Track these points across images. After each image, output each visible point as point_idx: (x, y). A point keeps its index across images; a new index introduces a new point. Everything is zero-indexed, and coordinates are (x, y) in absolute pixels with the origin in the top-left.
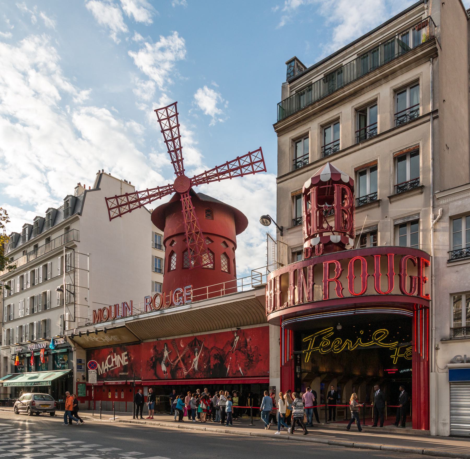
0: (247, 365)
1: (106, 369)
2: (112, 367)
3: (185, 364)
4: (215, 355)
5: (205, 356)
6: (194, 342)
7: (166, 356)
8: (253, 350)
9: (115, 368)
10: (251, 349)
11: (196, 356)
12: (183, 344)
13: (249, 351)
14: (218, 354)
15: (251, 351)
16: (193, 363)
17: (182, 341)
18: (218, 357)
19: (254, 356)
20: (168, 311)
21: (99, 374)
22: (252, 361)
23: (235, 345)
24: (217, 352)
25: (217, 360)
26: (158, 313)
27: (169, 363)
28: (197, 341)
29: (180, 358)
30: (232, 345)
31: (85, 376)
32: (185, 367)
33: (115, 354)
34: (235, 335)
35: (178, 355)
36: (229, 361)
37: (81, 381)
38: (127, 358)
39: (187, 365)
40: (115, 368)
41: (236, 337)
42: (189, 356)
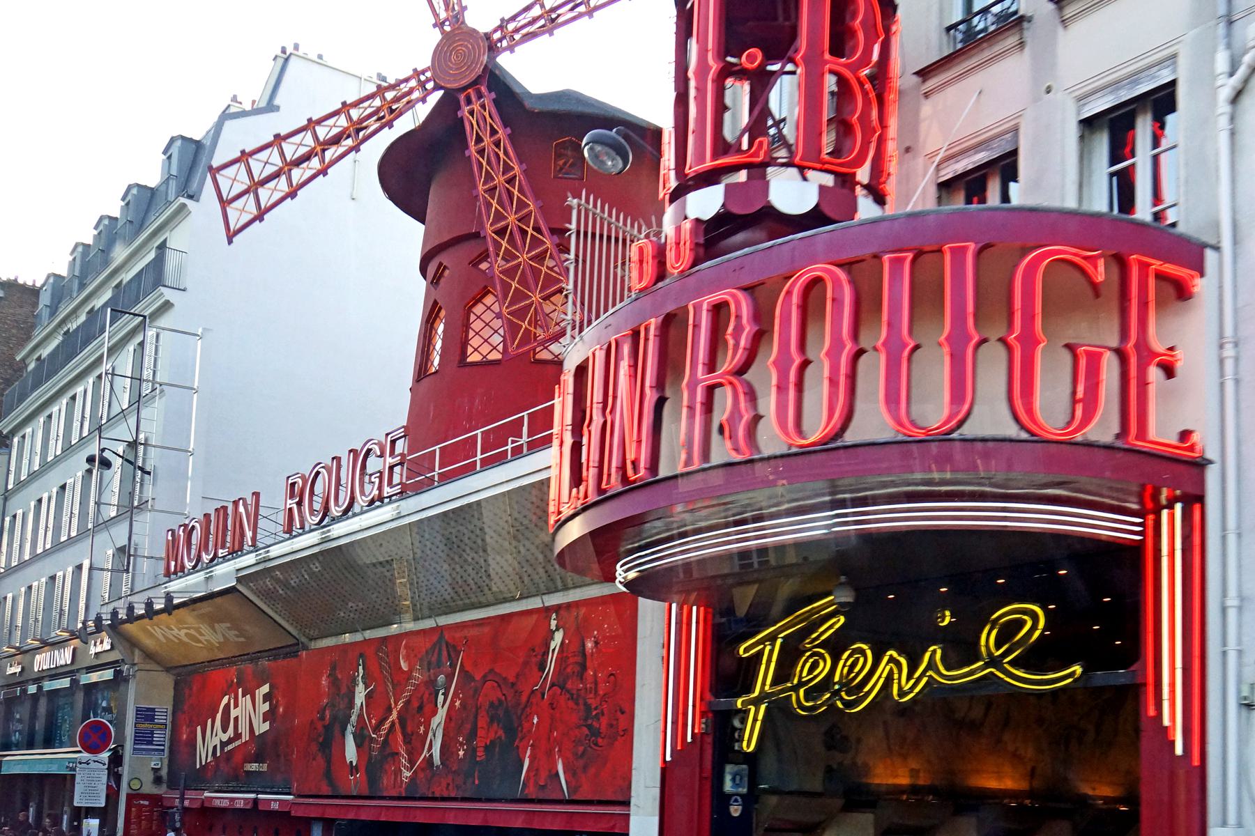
2: (230, 741)
3: (408, 739)
7: (359, 705)
9: (238, 743)
11: (439, 706)
12: (407, 658)
14: (500, 701)
16: (430, 734)
18: (501, 713)
21: (198, 767)
24: (499, 694)
27: (365, 732)
29: (394, 715)
31: (164, 773)
33: (240, 690)
37: (149, 788)
38: (266, 707)
39: (415, 742)
40: (238, 743)
42: (420, 708)
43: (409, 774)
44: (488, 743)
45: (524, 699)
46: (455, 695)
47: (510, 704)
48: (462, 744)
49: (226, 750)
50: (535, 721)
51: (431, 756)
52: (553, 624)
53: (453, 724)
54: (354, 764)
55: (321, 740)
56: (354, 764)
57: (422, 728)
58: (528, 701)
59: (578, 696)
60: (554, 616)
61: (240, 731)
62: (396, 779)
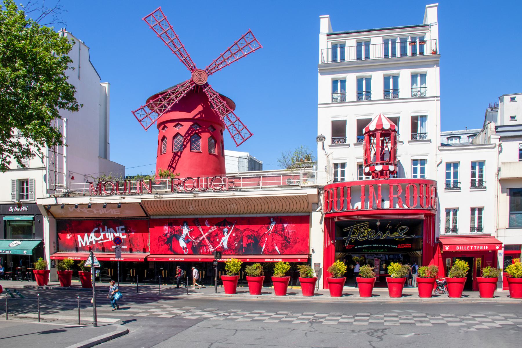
1: (91, 242)
2: (101, 240)
4: (248, 235)
5: (236, 235)
9: (106, 241)
14: (252, 235)
16: (222, 241)
17: (208, 221)
19: (291, 238)
20: (202, 196)
26: (191, 195)
27: (190, 240)
29: (204, 236)
32: (211, 245)
33: (106, 227)
35: (203, 233)
40: (106, 241)
42: (217, 235)
43: (213, 250)
44: (248, 243)
45: (261, 235)
46: (233, 232)
48: (236, 243)
49: (99, 242)
50: (266, 239)
51: (223, 246)
52: (272, 220)
53: (232, 239)
54: (185, 247)
55: (166, 241)
56: (185, 247)
57: (218, 240)
58: (263, 235)
59: (282, 235)
60: (272, 219)
61: (107, 237)
62: (207, 250)
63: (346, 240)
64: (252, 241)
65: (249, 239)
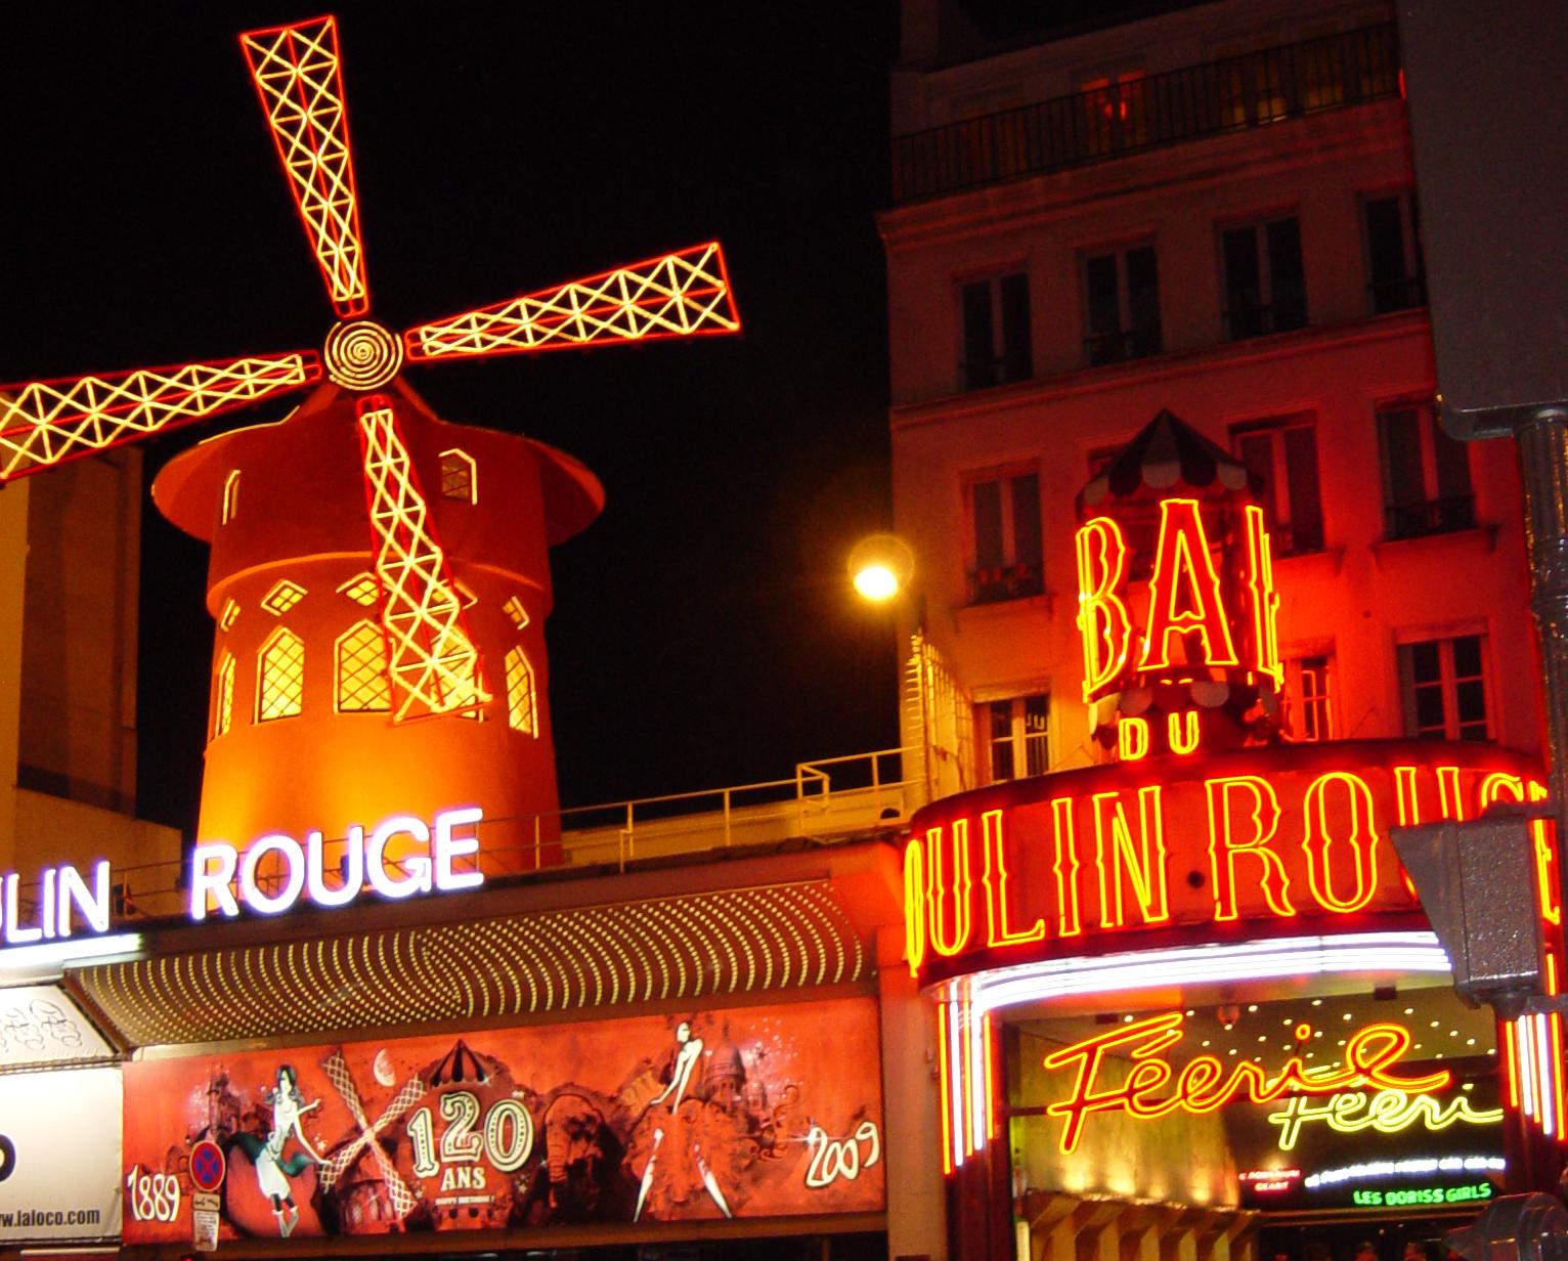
0: (745, 1162)
4: (573, 1121)
6: (452, 1058)
8: (773, 1102)
10: (764, 1096)
13: (755, 1103)
14: (589, 1118)
15: (765, 1104)
22: (772, 1146)
23: (682, 1077)
24: (586, 1108)
25: (582, 1144)
28: (466, 1060)
30: (666, 1077)
34: (683, 1033)
36: (649, 1148)
41: (685, 1044)
44: (571, 1161)
47: (608, 1120)
63: (1065, 1117)
64: (592, 1150)
65: (575, 1137)
